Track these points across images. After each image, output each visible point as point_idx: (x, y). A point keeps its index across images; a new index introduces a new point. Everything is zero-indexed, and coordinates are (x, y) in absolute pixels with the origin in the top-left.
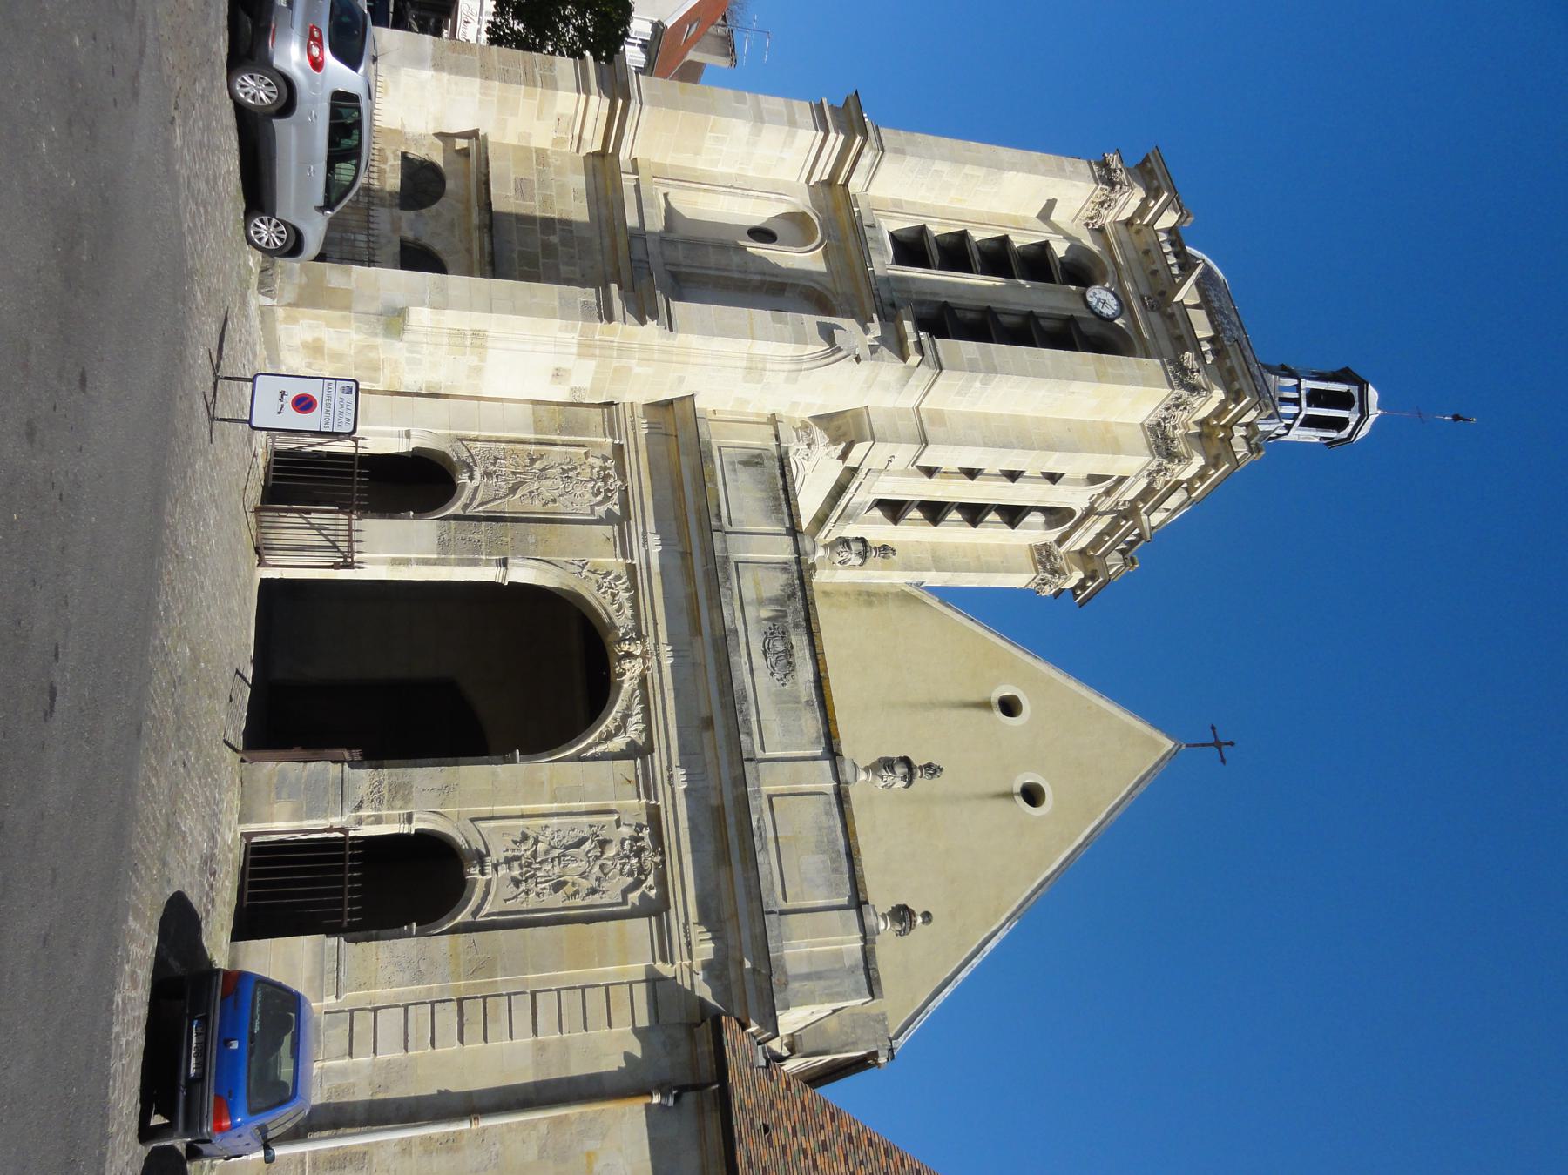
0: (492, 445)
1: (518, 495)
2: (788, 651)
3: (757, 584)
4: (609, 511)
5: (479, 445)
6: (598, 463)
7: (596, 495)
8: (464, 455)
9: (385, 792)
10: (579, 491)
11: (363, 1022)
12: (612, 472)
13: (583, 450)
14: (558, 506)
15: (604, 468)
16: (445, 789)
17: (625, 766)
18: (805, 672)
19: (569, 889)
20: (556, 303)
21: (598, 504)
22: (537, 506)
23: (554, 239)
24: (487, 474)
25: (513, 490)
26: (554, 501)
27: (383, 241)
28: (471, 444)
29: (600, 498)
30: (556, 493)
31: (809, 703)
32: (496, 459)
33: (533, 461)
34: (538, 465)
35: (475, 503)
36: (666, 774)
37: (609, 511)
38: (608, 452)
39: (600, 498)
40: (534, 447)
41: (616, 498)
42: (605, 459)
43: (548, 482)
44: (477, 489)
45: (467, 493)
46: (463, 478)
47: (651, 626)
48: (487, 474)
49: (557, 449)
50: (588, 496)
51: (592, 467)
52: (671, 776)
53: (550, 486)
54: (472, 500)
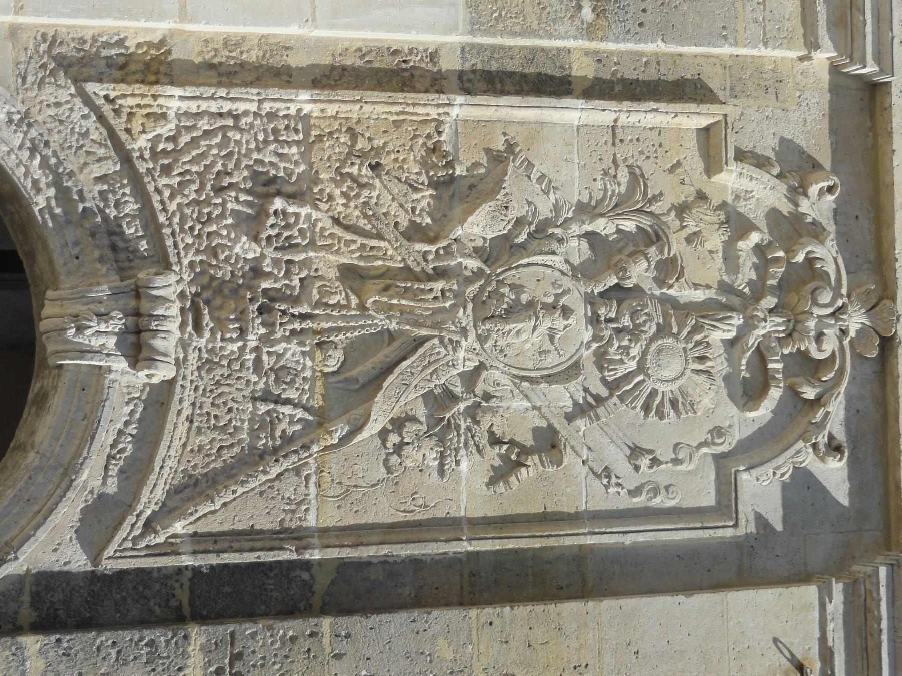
0: (247, 101)
1: (380, 415)
4: (802, 489)
5: (174, 99)
6: (762, 193)
7: (749, 392)
8: (92, 173)
10: (669, 371)
12: (827, 254)
13: (691, 119)
14: (570, 484)
15: (791, 228)
21: (759, 446)
22: (465, 487)
24: (212, 298)
25: (353, 390)
26: (549, 443)
28: (131, 95)
29: (764, 411)
30: (562, 396)
32: (266, 186)
33: (456, 192)
34: (478, 226)
35: (151, 498)
37: (802, 489)
38: (807, 122)
39: (764, 411)
40: (461, 108)
41: (835, 415)
42: (795, 167)
43: (524, 339)
44: (159, 399)
45: (117, 416)
46: (84, 337)
48: (212, 298)
49: (572, 113)
50: (712, 401)
51: (737, 225)
53: (524, 362)
54: (136, 471)
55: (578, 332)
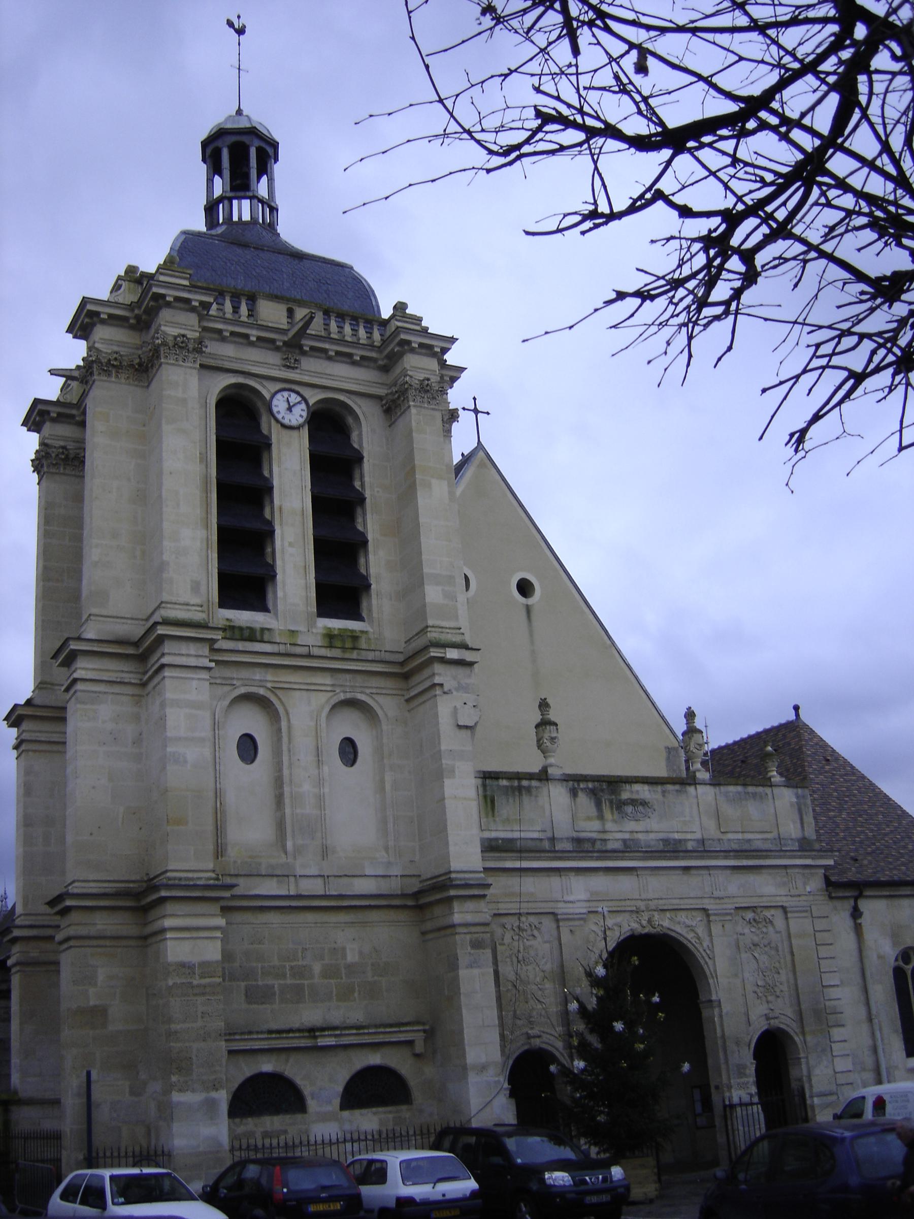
2: (633, 802)
3: (589, 819)
9: (742, 1080)
11: (841, 1079)
16: (738, 1043)
17: (716, 929)
18: (643, 792)
19: (777, 965)
20: (476, 971)
23: (317, 968)
27: (347, 1127)
31: (664, 793)
36: (718, 901)
46: (536, 1043)
47: (628, 903)
52: (719, 898)
55: (529, 968)
